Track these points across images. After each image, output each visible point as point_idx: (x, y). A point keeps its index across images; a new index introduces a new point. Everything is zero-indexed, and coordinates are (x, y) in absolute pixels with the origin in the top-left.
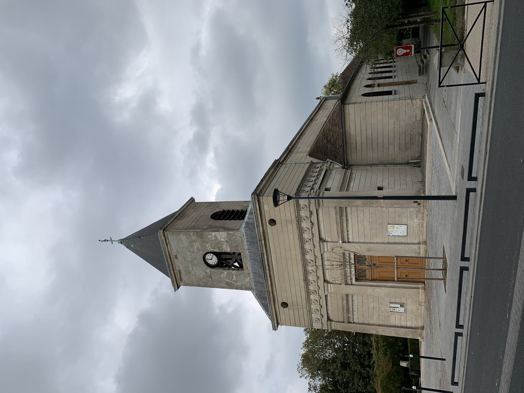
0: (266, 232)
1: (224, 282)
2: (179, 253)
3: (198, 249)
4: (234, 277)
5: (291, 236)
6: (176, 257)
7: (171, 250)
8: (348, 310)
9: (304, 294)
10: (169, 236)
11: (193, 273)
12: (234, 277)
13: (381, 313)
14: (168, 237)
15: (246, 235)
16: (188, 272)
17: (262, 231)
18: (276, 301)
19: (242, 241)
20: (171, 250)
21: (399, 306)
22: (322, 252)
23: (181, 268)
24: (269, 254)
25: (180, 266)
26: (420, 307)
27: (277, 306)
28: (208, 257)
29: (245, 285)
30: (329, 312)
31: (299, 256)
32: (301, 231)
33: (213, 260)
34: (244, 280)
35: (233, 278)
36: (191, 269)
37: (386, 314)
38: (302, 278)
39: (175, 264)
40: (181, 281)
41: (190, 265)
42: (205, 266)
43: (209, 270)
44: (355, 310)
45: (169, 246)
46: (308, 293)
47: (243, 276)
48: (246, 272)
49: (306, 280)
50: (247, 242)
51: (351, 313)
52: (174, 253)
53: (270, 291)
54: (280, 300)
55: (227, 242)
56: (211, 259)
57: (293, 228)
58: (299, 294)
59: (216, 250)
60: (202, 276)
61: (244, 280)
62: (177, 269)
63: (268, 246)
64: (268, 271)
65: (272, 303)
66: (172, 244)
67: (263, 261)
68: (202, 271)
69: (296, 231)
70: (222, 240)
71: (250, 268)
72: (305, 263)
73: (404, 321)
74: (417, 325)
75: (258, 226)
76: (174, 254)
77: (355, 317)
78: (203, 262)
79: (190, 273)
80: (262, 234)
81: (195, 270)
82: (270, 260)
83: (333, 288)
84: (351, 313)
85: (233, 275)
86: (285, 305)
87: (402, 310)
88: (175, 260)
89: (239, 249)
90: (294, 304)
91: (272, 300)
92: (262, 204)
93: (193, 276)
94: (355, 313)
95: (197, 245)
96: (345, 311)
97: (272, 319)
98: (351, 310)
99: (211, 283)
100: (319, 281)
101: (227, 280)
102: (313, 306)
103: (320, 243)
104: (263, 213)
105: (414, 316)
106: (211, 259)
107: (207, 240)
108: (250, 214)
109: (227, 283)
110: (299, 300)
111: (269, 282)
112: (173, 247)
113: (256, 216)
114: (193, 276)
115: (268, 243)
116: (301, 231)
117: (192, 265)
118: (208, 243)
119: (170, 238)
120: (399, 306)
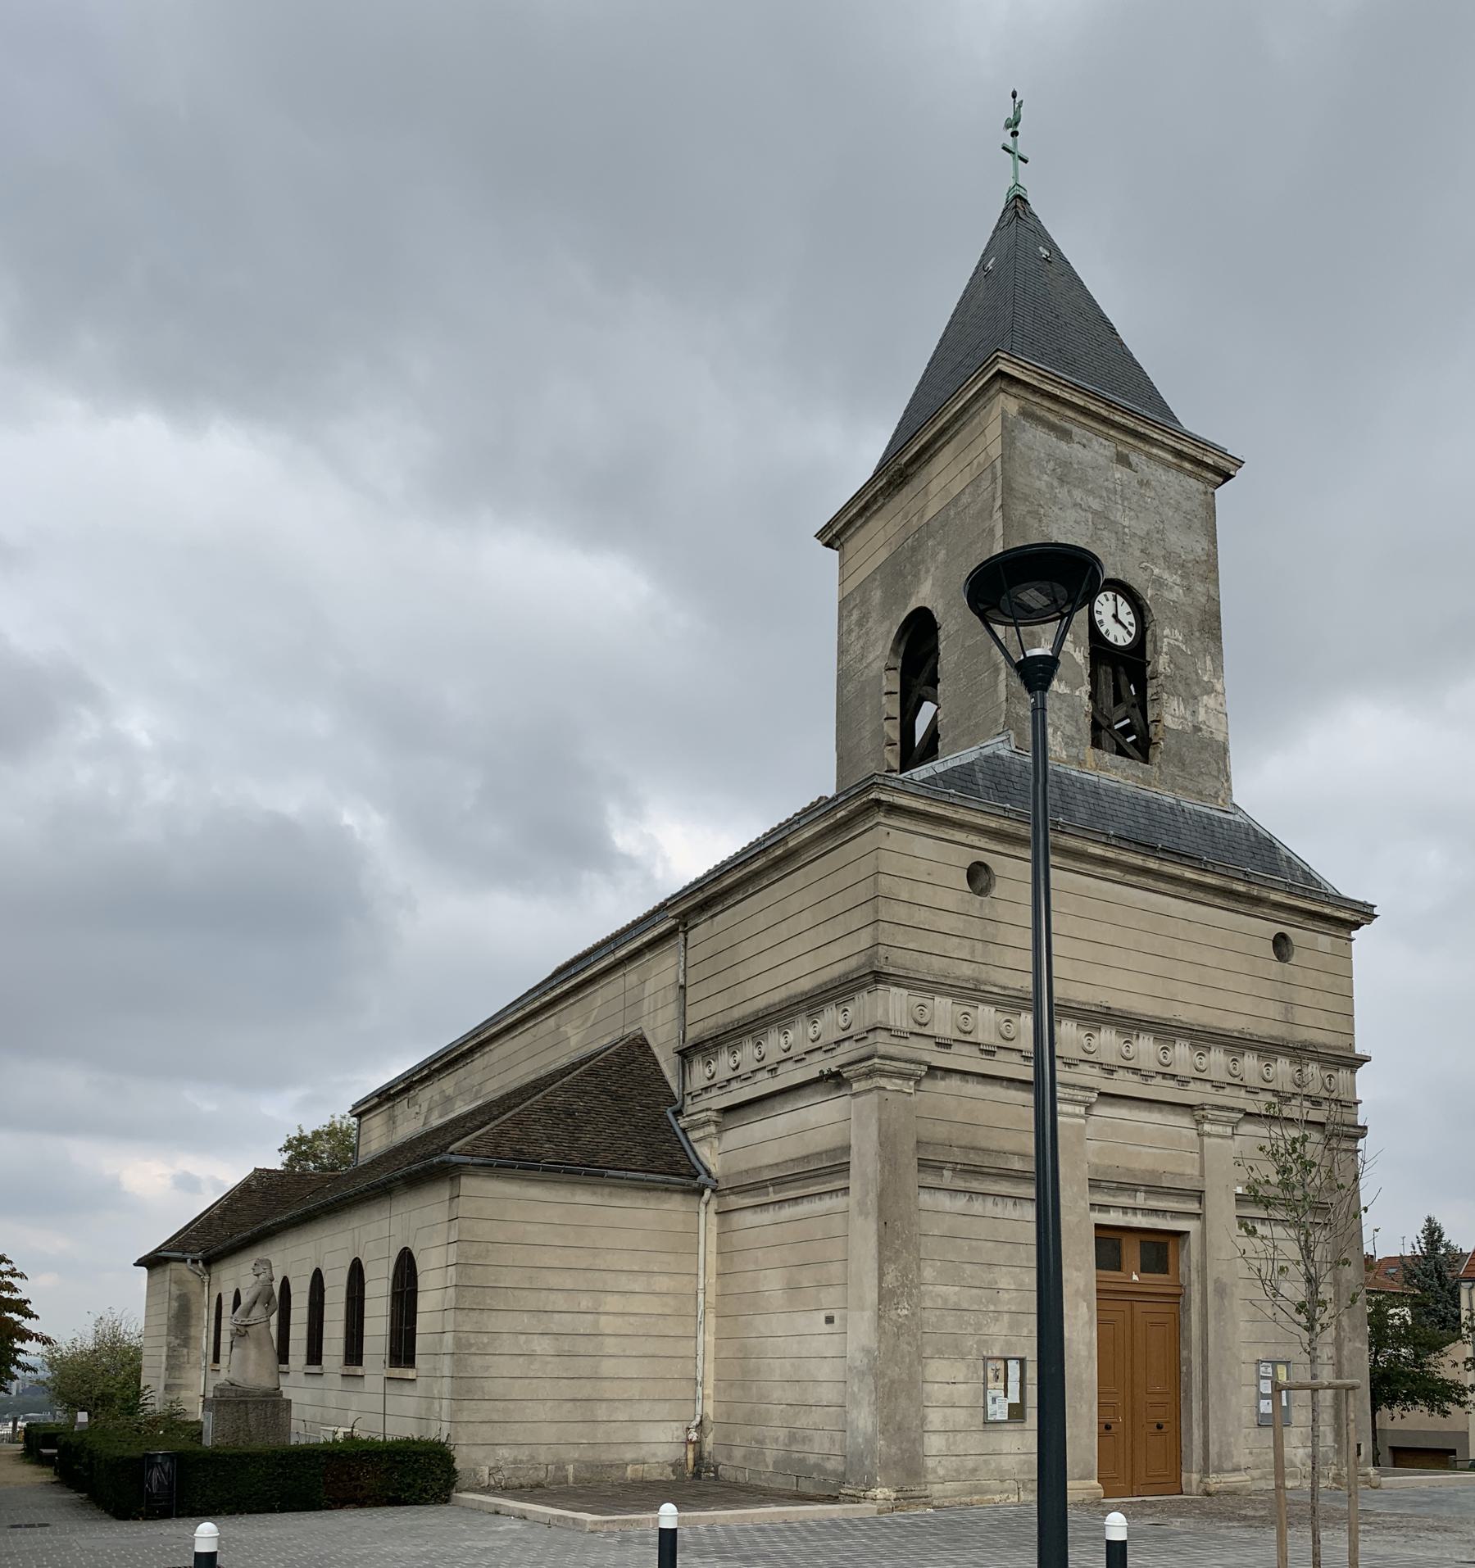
3: (1159, 583)
8: (976, 1172)
13: (970, 1318)
14: (1197, 477)
21: (1014, 1398)
22: (1210, 1114)
26: (1010, 1484)
27: (974, 839)
30: (954, 1083)
37: (970, 1342)
44: (978, 1206)
51: (960, 1184)
56: (1115, 616)
64: (1138, 860)
65: (1006, 825)
67: (1180, 856)
72: (1165, 1031)
73: (945, 1421)
74: (930, 1477)
77: (945, 1202)
83: (1072, 1126)
84: (960, 1184)
85: (1074, 687)
87: (999, 1411)
90: (991, 928)
94: (960, 1203)
96: (975, 1159)
98: (975, 1185)
100: (1096, 1071)
103: (1240, 1110)
105: (970, 1463)
106: (1115, 616)
111: (1097, 850)
120: (1014, 1398)
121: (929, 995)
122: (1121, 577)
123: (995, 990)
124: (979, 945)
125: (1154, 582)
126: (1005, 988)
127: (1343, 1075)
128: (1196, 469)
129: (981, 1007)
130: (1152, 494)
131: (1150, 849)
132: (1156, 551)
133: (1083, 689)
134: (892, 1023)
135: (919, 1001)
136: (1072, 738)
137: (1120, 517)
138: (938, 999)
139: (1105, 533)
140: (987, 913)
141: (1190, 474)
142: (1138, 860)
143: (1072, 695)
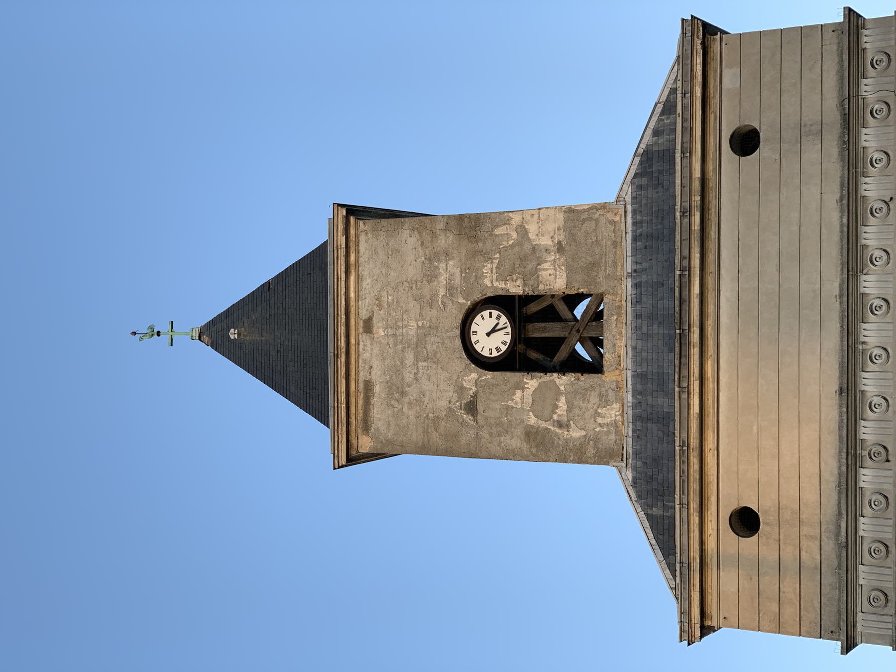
0: (712, 182)
1: (519, 431)
2: (380, 307)
3: (451, 289)
4: (562, 403)
5: (812, 192)
6: (368, 326)
7: (357, 298)
9: (832, 466)
10: (363, 238)
11: (413, 393)
12: (562, 403)
14: (357, 244)
15: (634, 212)
16: (397, 390)
17: (697, 173)
18: (713, 499)
19: (615, 244)
20: (357, 298)
23: (377, 376)
24: (710, 323)
25: (376, 364)
28: (483, 322)
29: (597, 440)
31: (833, 285)
32: (853, 163)
33: (492, 335)
34: (597, 414)
35: (556, 407)
36: (409, 377)
38: (832, 384)
39: (358, 355)
40: (366, 428)
41: (410, 358)
42: (461, 361)
43: (473, 376)
45: (352, 278)
46: (852, 454)
47: (594, 398)
48: (609, 376)
49: (850, 393)
50: (635, 239)
52: (363, 308)
53: (694, 442)
54: (727, 498)
55: (560, 248)
57: (823, 159)
58: (810, 467)
59: (516, 288)
60: (443, 403)
61: (597, 414)
62: (363, 376)
63: (712, 246)
65: (694, 505)
66: (365, 270)
67: (684, 301)
68: (445, 382)
69: (835, 169)
70: (546, 241)
71: (627, 362)
75: (687, 151)
76: (364, 314)
78: (458, 342)
79: (403, 393)
80: (697, 185)
81: (424, 380)
82: (711, 308)
85: (558, 393)
86: (746, 521)
88: (364, 338)
89: (601, 278)
90: (786, 515)
91: (695, 486)
92: (714, 65)
93: (410, 403)
95: (450, 271)
97: (681, 594)
99: (472, 433)
101: (533, 420)
102: (865, 526)
104: (714, 102)
107: (489, 245)
108: (662, 113)
109: (531, 434)
110: (810, 496)
112: (367, 283)
113: (688, 119)
114: (410, 403)
115: (713, 234)
116: (853, 163)
117: (417, 360)
118: (491, 260)
119: (363, 247)
121: (859, 590)
122: (458, 332)
123: (843, 525)
124: (805, 530)
125: (452, 295)
126: (839, 514)
127: (869, 41)
128: (352, 249)
129: (861, 533)
130: (385, 294)
131: (684, 339)
132: (426, 292)
133: (557, 381)
134: (890, 632)
135: (866, 606)
136: (601, 395)
137: (412, 329)
138: (861, 581)
139: (429, 347)
140: (773, 518)
141: (357, 252)
142: (695, 352)
143: (567, 394)
